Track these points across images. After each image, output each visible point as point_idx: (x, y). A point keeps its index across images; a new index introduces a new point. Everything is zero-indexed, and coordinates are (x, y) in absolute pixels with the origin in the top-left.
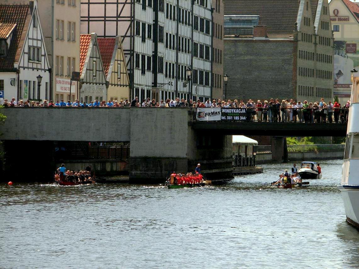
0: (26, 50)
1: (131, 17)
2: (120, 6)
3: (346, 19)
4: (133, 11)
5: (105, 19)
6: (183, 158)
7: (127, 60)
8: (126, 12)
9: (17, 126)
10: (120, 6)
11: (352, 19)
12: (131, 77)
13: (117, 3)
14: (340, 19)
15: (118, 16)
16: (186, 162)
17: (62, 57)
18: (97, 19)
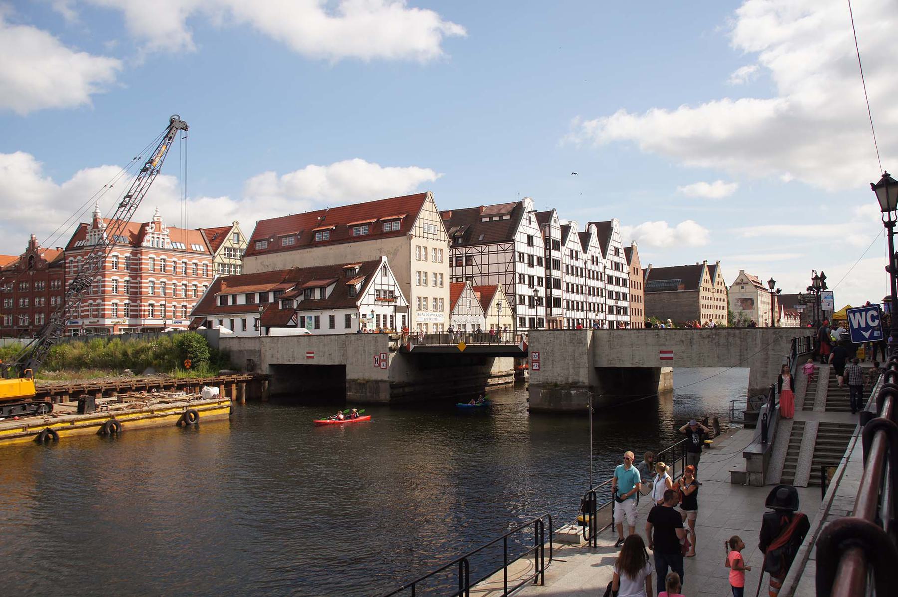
0: (372, 291)
1: (513, 271)
2: (507, 264)
3: (747, 283)
4: (514, 266)
5: (498, 273)
6: (385, 382)
7: (512, 299)
8: (510, 269)
9: (278, 352)
10: (507, 264)
11: (750, 283)
12: (514, 310)
13: (505, 263)
14: (744, 283)
15: (506, 271)
16: (387, 386)
17: (426, 298)
18: (493, 274)
